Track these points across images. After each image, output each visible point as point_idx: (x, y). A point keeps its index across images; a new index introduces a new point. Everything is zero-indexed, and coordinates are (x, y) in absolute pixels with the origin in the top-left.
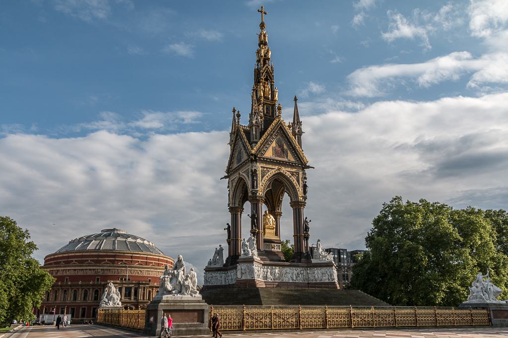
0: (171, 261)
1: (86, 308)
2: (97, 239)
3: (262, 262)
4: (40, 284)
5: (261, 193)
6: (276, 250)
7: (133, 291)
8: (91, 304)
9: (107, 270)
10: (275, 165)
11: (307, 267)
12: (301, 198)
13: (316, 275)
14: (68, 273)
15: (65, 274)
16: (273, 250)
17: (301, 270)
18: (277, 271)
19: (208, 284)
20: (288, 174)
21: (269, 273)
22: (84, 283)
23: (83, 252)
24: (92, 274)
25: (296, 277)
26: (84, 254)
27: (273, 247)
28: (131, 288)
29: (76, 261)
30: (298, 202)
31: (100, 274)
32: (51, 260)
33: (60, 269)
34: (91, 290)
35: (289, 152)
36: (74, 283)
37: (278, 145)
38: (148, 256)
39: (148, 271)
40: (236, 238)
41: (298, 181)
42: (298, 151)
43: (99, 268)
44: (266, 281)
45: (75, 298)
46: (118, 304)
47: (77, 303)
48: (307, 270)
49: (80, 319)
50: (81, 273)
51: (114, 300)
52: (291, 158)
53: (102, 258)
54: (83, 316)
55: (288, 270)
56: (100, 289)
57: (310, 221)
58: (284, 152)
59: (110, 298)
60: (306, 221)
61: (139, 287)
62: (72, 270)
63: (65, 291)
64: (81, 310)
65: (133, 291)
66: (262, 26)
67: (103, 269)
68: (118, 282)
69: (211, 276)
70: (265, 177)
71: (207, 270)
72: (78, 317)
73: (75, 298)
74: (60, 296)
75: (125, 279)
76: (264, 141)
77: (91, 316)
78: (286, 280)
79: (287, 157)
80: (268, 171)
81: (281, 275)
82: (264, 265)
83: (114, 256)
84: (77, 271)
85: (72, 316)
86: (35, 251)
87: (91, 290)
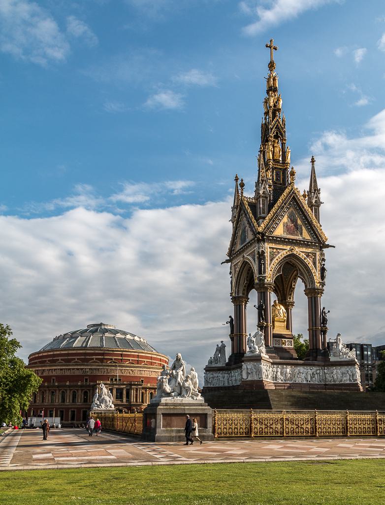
0: (165, 359)
1: (76, 410)
2: (83, 335)
3: (271, 361)
4: (25, 385)
5: (269, 280)
6: (286, 346)
7: (125, 392)
8: (81, 406)
9: (95, 369)
10: (287, 245)
11: (324, 366)
12: (318, 285)
13: (335, 375)
14: (54, 373)
15: (51, 374)
16: (283, 346)
17: (317, 370)
18: (288, 370)
19: (209, 386)
20: (302, 256)
21: (279, 373)
22: (72, 384)
23: (69, 350)
24: (79, 374)
25: (311, 378)
26: (71, 352)
27: (283, 343)
28: (123, 389)
29: (61, 359)
30: (314, 289)
31: (89, 374)
32: (35, 358)
33: (46, 368)
34: (80, 391)
35: (303, 228)
36: (61, 384)
37: (291, 219)
38: (140, 354)
39: (140, 371)
40: (240, 333)
41: (314, 263)
42: (315, 227)
44: (275, 382)
45: (63, 400)
46: (111, 407)
47: (66, 405)
48: (325, 369)
49: (70, 422)
50: (68, 373)
51: (106, 402)
52: (306, 235)
53: (89, 356)
54: (73, 419)
55: (301, 369)
56: (89, 390)
57: (329, 312)
58: (297, 228)
59: (102, 401)
60: (323, 312)
63: (53, 392)
65: (125, 392)
66: (271, 66)
67: (92, 369)
68: (109, 382)
69: (211, 376)
70: (275, 259)
71: (208, 369)
72: (68, 421)
73: (63, 400)
75: (116, 380)
76: (273, 216)
78: (299, 381)
79: (301, 234)
80: (279, 253)
81: (293, 374)
82: (273, 364)
83: (103, 354)
84: (63, 370)
85: (62, 420)
86: (18, 350)
87: (80, 391)
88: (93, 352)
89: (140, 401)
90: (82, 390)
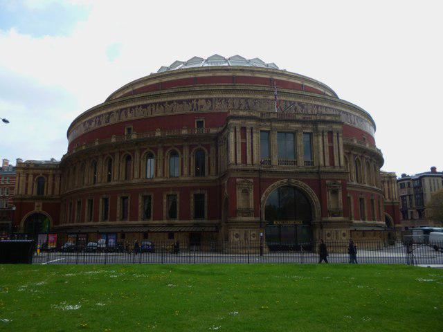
8: (188, 185)
9: (220, 100)
14: (131, 116)
15: (124, 119)
31: (205, 109)
34: (186, 151)
38: (305, 84)
39: (318, 106)
43: (200, 96)
47: (156, 183)
49: (165, 221)
50: (159, 112)
56: (208, 147)
61: (316, 130)
62: (139, 106)
63: (129, 158)
64: (165, 201)
67: (211, 99)
72: (162, 219)
74: (116, 169)
77: (192, 214)
87: (186, 151)
88: (211, 75)
89: (342, 163)
90: (191, 147)
